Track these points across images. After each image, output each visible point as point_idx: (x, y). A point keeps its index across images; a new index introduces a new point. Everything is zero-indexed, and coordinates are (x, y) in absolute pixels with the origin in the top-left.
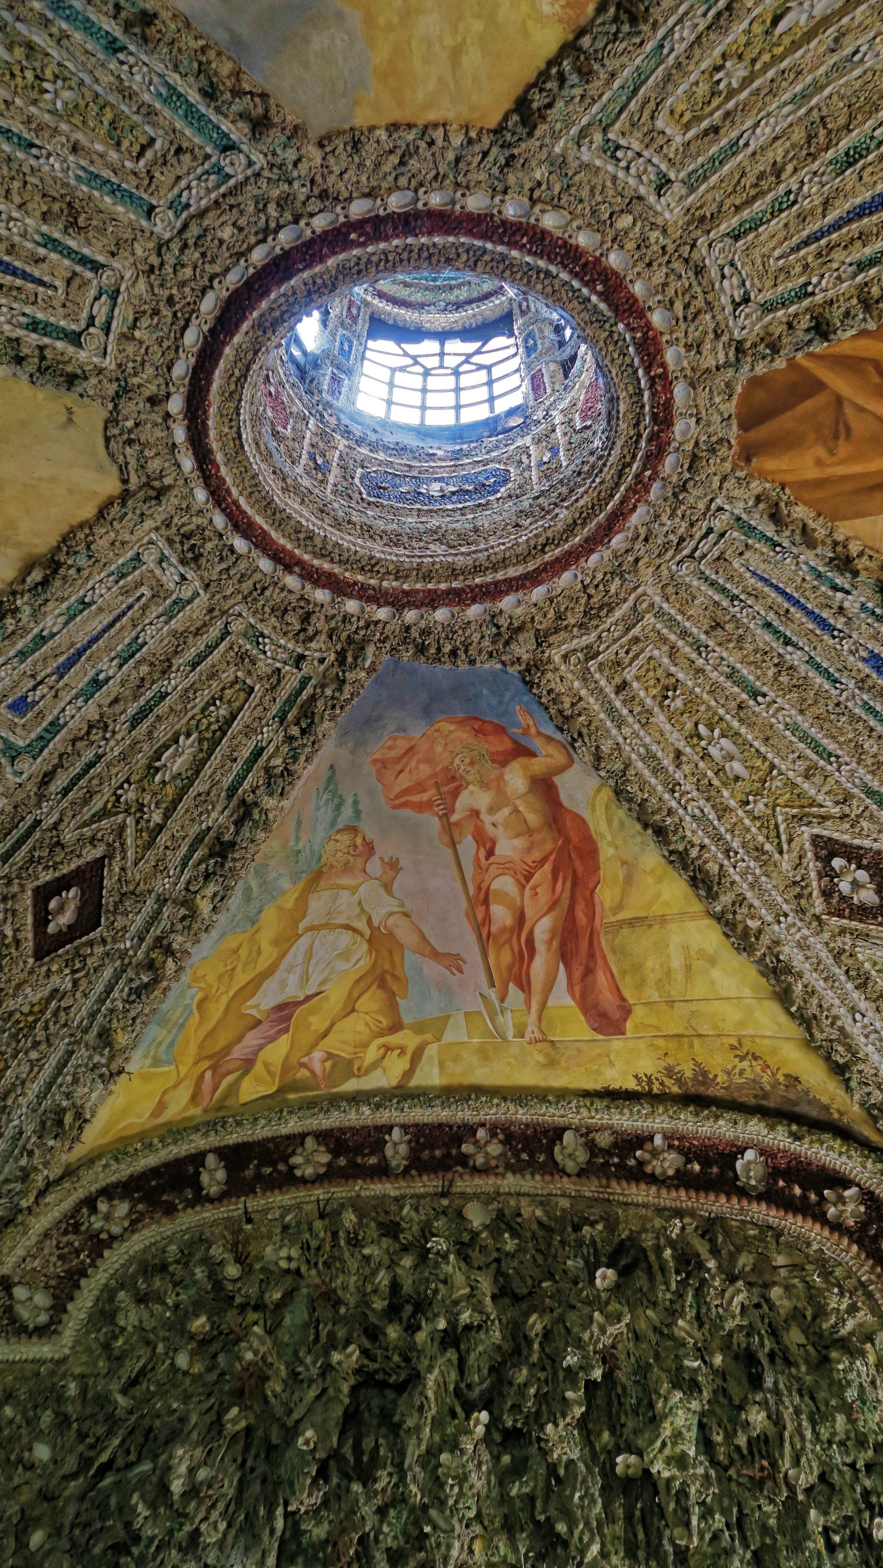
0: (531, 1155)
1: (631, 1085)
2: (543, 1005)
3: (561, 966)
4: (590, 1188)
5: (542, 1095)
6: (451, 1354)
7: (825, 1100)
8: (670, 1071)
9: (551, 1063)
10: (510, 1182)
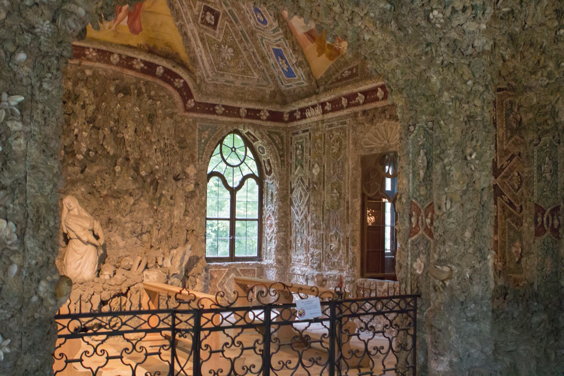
0: (104, 57)
1: (136, 45)
2: (119, 23)
3: (127, 17)
4: (118, 69)
5: (111, 44)
6: (84, 110)
7: (183, 59)
8: (147, 45)
9: (115, 36)
10: (97, 64)
